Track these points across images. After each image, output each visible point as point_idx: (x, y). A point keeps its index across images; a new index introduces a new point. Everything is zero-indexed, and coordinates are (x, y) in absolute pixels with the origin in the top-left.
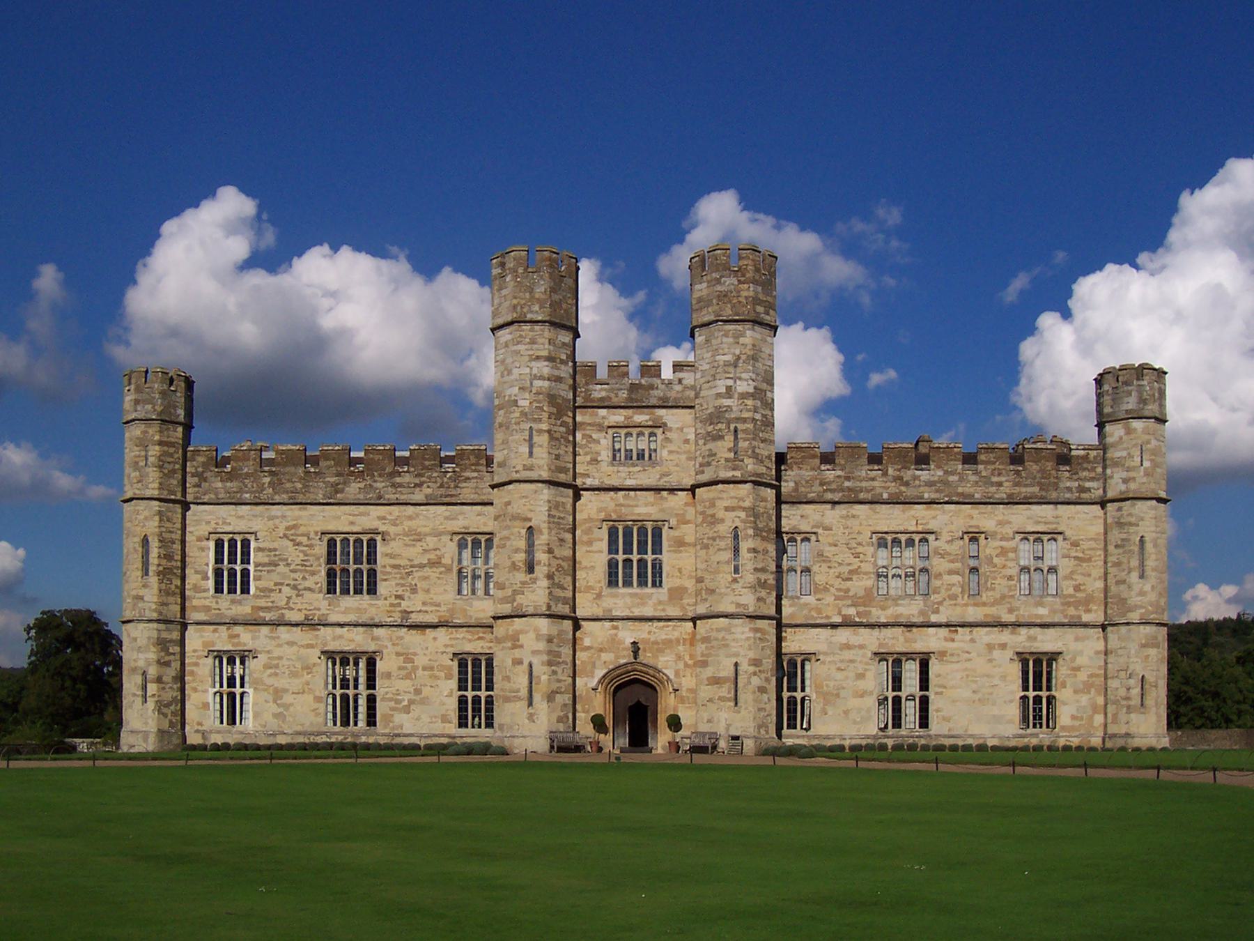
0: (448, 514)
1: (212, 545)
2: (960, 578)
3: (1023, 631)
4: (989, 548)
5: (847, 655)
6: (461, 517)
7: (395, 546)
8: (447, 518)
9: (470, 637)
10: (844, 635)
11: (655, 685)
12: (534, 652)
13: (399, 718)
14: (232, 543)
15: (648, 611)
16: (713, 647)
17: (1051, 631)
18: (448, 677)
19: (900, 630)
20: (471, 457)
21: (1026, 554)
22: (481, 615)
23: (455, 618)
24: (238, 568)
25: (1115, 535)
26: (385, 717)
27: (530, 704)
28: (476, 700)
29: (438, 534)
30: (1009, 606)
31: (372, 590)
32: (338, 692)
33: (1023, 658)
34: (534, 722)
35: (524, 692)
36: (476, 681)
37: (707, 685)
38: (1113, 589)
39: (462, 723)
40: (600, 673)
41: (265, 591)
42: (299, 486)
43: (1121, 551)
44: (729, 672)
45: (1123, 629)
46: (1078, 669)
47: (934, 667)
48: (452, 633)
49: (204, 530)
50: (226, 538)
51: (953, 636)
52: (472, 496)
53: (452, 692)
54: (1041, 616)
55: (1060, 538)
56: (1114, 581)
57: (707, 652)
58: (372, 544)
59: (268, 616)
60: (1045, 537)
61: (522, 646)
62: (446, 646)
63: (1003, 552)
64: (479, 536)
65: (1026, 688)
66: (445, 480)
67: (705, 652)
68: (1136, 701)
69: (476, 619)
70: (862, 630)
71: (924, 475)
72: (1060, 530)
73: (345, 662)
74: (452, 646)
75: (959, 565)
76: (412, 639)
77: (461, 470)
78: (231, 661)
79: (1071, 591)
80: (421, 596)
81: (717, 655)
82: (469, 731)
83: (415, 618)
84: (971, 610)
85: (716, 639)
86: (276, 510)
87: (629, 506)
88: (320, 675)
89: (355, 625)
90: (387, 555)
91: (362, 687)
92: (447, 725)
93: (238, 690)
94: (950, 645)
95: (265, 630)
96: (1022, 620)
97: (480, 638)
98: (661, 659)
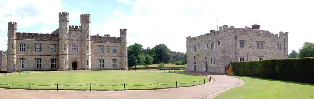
1: (20, 45)
3: (113, 57)
4: (110, 48)
5: (95, 59)
7: (43, 46)
10: (94, 57)
13: (44, 67)
14: (23, 45)
15: (77, 54)
18: (50, 61)
19: (100, 57)
21: (113, 48)
24: (23, 48)
26: (43, 67)
27: (65, 65)
28: (54, 64)
29: (49, 44)
31: (41, 51)
32: (37, 64)
33: (113, 59)
36: (54, 62)
38: (122, 53)
39: (52, 67)
40: (71, 61)
41: (27, 51)
42: (32, 38)
44: (86, 61)
46: (118, 61)
47: (104, 61)
49: (19, 43)
50: (22, 44)
58: (41, 45)
59: (27, 54)
63: (111, 48)
68: (125, 65)
70: (97, 57)
71: (103, 39)
73: (37, 60)
76: (46, 57)
78: (22, 60)
79: (118, 52)
80: (47, 52)
82: (53, 68)
83: (46, 54)
84: (108, 54)
86: (28, 41)
88: (34, 62)
89: (39, 55)
90: (43, 47)
91: (39, 63)
93: (23, 63)
95: (27, 56)
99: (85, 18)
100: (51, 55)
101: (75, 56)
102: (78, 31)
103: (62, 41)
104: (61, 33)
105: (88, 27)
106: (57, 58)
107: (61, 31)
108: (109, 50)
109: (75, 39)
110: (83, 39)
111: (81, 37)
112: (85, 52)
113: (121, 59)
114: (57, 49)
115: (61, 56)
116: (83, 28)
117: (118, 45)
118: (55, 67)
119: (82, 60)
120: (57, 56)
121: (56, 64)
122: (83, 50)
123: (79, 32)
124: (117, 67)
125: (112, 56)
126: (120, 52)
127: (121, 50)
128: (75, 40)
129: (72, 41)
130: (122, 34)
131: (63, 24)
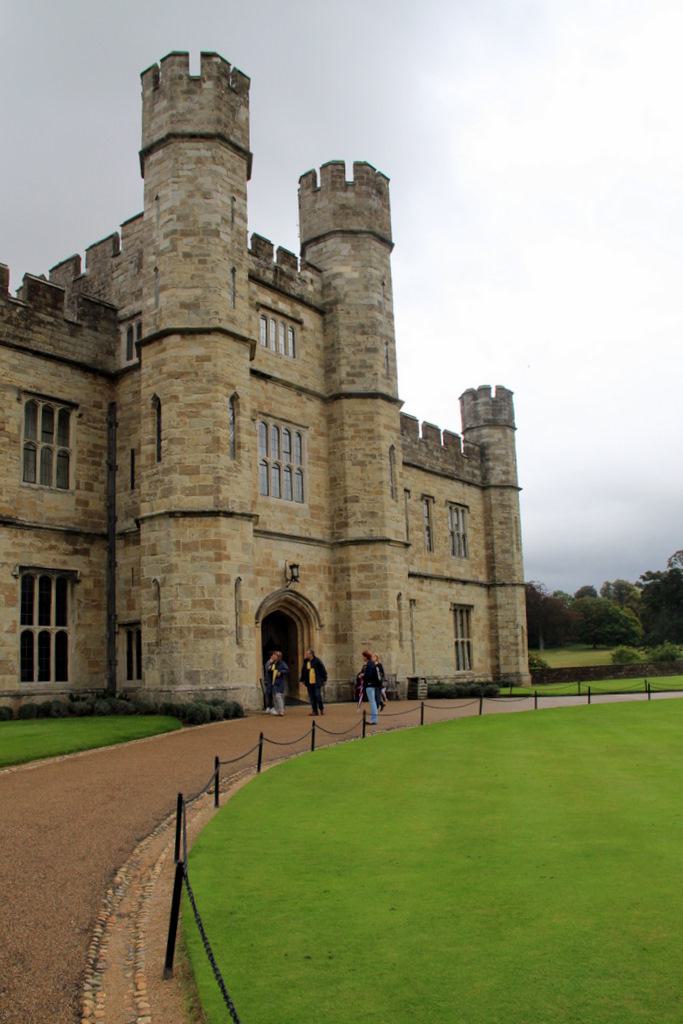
0: (15, 362)
2: (420, 534)
3: (454, 585)
4: (436, 509)
6: (32, 372)
8: (14, 368)
9: (40, 544)
11: (293, 617)
12: (242, 568)
15: (296, 531)
16: (377, 577)
17: (467, 588)
18: (9, 603)
20: (48, 296)
22: (52, 514)
23: (20, 514)
25: (498, 514)
28: (45, 636)
30: (446, 563)
34: (243, 666)
35: (231, 626)
37: (369, 620)
38: (500, 556)
39: (27, 676)
43: (504, 527)
44: (393, 607)
45: (509, 589)
48: (16, 536)
51: (420, 585)
52: (47, 347)
53: (15, 626)
54: (459, 573)
55: (466, 510)
56: (500, 550)
57: (368, 582)
60: (460, 509)
61: (228, 558)
62: (8, 554)
64: (53, 404)
65: (456, 637)
66: (14, 315)
67: (364, 582)
69: (48, 519)
72: (467, 504)
74: (15, 555)
75: (421, 523)
77: (35, 307)
81: (385, 586)
82: (36, 685)
84: (430, 563)
85: (380, 567)
87: (278, 402)
92: (8, 677)
94: (420, 593)
96: (454, 576)
97: (52, 548)
98: (309, 589)
99: (356, 193)
100: (26, 518)
101: (287, 545)
102: (300, 300)
103: (200, 351)
104: (189, 268)
105: (385, 283)
106: (76, 564)
107: (185, 244)
108: (434, 529)
109: (276, 374)
110: (346, 388)
111: (329, 369)
112: (373, 514)
113: (493, 607)
114: (81, 461)
115: (192, 531)
116: (350, 281)
117: (472, 497)
118: (62, 676)
119: (342, 595)
120: (82, 545)
121: (72, 640)
122: (351, 493)
123: (308, 318)
124: (476, 664)
125: (450, 580)
126: (483, 553)
127: (488, 534)
128: (287, 385)
129: (260, 384)
130: (492, 424)
131: (213, 173)
